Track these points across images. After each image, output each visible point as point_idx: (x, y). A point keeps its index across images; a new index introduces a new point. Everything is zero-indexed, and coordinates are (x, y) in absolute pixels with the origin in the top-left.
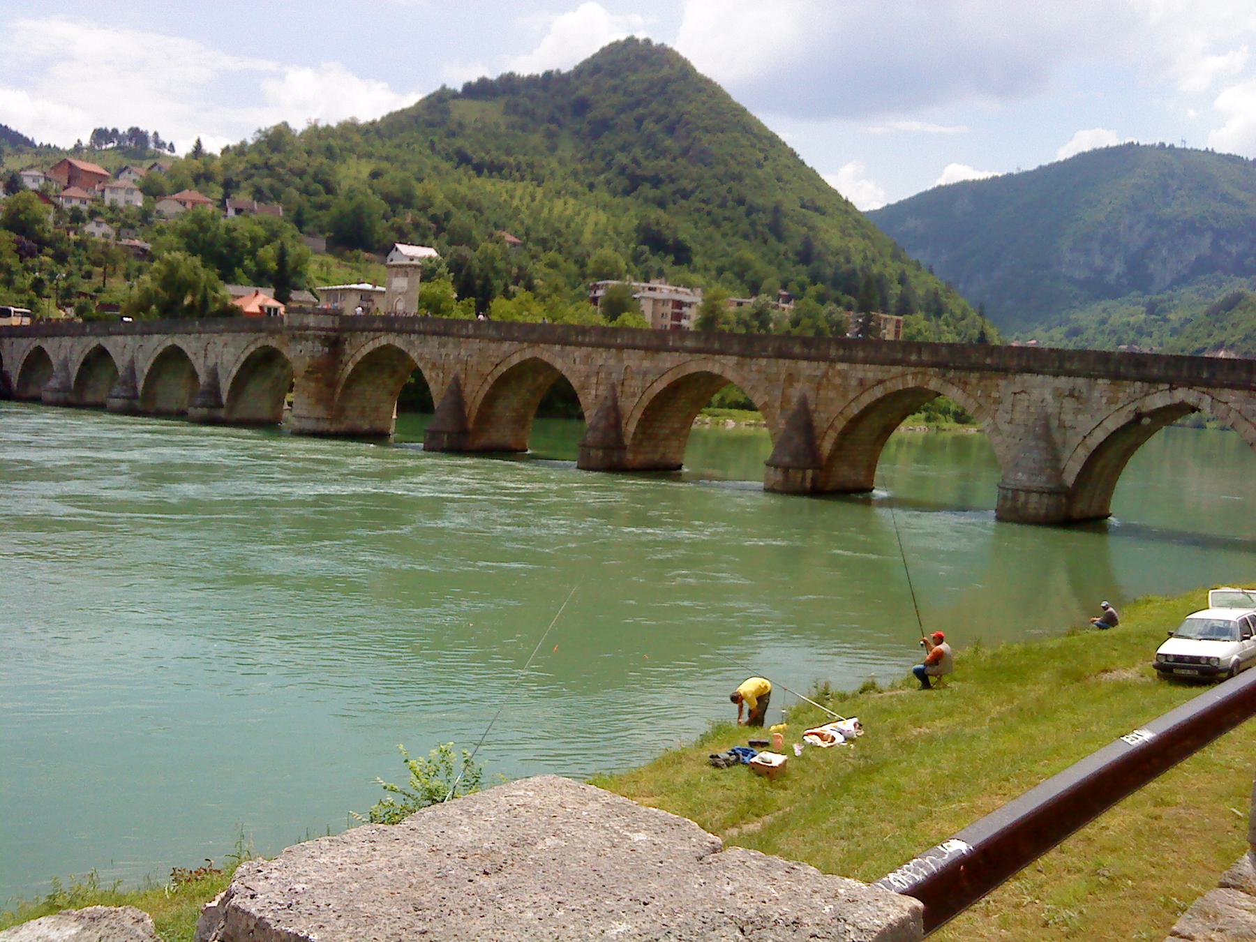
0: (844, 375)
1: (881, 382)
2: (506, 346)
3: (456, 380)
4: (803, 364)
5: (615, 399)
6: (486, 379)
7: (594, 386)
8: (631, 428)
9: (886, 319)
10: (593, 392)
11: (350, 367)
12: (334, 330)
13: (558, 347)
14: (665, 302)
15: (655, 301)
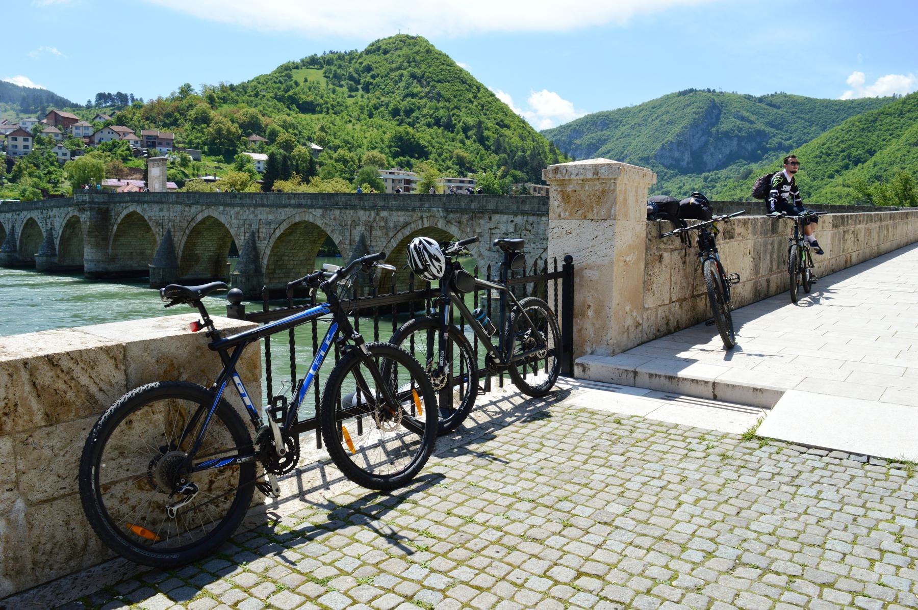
0: (386, 220)
1: (406, 224)
2: (194, 209)
3: (169, 232)
4: (361, 213)
5: (254, 242)
6: (185, 232)
7: (243, 234)
8: (265, 262)
9: (539, 188)
10: (242, 238)
11: (115, 227)
12: (104, 203)
13: (221, 208)
14: (400, 181)
15: (393, 181)
